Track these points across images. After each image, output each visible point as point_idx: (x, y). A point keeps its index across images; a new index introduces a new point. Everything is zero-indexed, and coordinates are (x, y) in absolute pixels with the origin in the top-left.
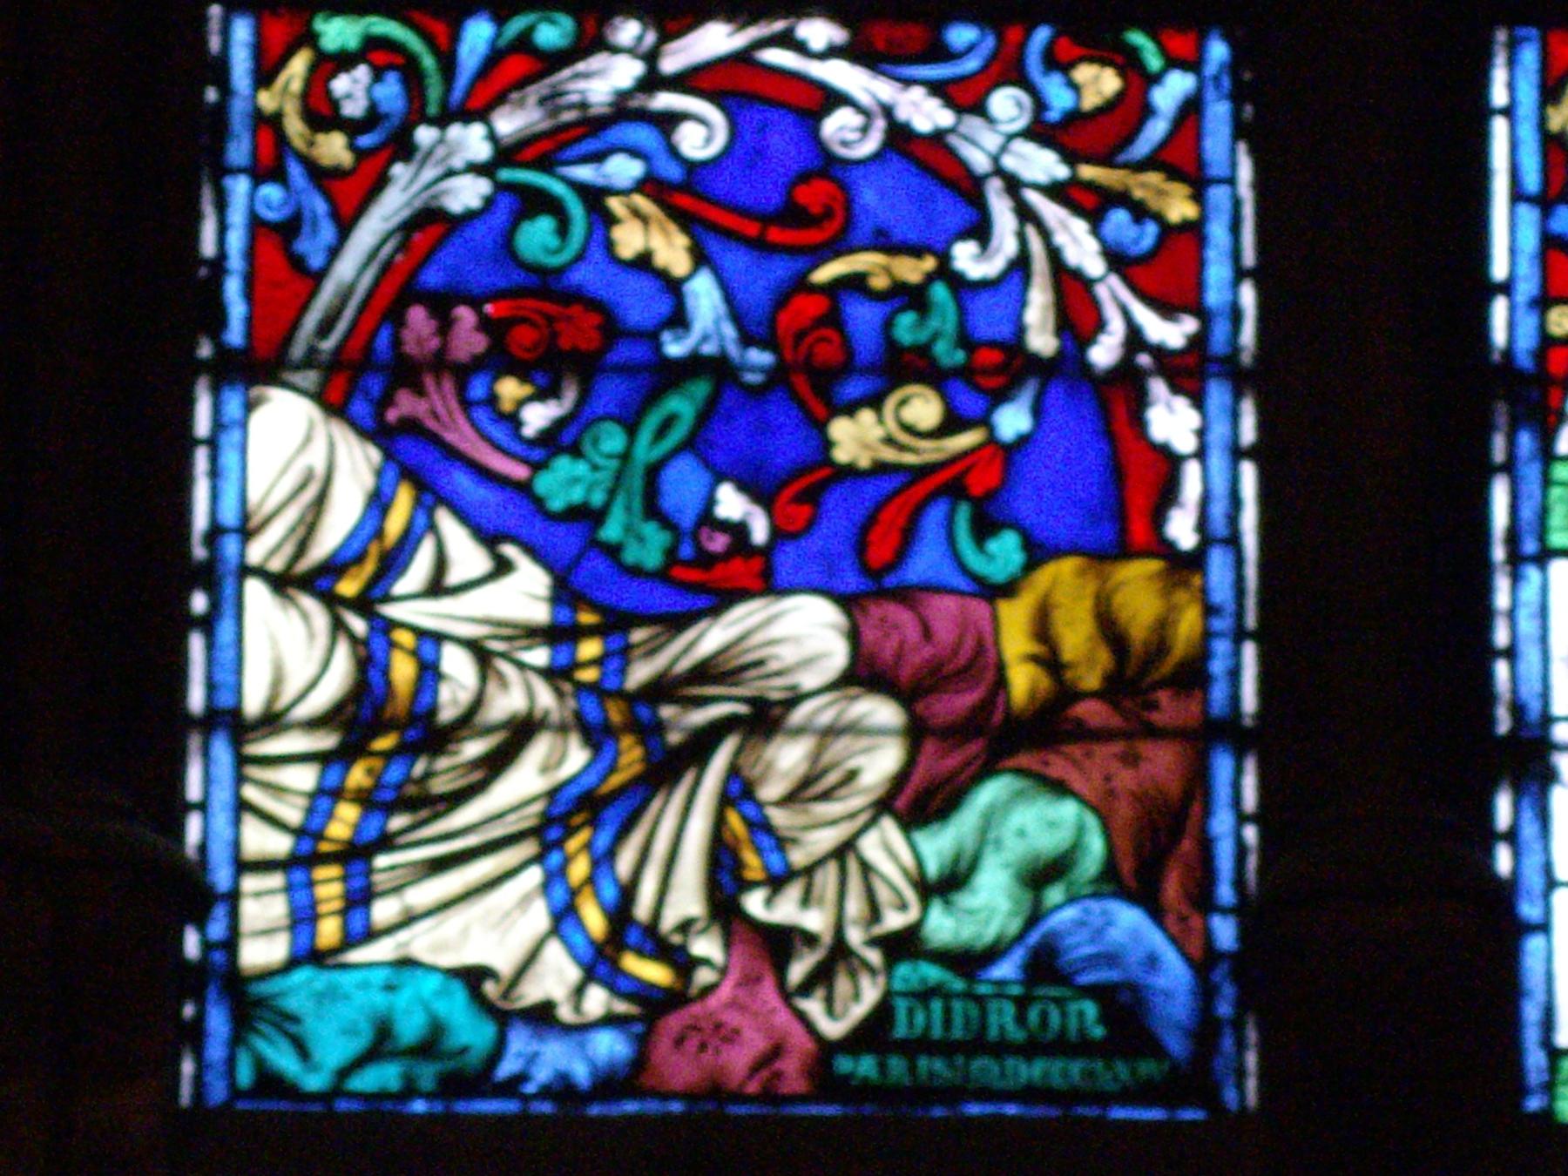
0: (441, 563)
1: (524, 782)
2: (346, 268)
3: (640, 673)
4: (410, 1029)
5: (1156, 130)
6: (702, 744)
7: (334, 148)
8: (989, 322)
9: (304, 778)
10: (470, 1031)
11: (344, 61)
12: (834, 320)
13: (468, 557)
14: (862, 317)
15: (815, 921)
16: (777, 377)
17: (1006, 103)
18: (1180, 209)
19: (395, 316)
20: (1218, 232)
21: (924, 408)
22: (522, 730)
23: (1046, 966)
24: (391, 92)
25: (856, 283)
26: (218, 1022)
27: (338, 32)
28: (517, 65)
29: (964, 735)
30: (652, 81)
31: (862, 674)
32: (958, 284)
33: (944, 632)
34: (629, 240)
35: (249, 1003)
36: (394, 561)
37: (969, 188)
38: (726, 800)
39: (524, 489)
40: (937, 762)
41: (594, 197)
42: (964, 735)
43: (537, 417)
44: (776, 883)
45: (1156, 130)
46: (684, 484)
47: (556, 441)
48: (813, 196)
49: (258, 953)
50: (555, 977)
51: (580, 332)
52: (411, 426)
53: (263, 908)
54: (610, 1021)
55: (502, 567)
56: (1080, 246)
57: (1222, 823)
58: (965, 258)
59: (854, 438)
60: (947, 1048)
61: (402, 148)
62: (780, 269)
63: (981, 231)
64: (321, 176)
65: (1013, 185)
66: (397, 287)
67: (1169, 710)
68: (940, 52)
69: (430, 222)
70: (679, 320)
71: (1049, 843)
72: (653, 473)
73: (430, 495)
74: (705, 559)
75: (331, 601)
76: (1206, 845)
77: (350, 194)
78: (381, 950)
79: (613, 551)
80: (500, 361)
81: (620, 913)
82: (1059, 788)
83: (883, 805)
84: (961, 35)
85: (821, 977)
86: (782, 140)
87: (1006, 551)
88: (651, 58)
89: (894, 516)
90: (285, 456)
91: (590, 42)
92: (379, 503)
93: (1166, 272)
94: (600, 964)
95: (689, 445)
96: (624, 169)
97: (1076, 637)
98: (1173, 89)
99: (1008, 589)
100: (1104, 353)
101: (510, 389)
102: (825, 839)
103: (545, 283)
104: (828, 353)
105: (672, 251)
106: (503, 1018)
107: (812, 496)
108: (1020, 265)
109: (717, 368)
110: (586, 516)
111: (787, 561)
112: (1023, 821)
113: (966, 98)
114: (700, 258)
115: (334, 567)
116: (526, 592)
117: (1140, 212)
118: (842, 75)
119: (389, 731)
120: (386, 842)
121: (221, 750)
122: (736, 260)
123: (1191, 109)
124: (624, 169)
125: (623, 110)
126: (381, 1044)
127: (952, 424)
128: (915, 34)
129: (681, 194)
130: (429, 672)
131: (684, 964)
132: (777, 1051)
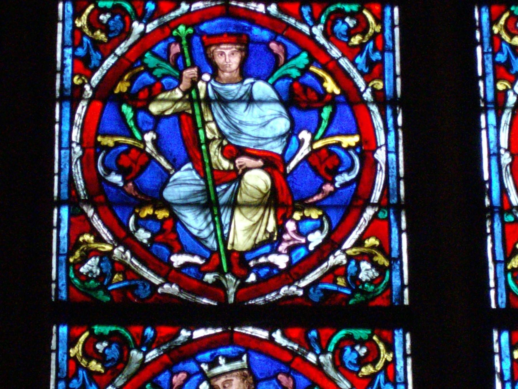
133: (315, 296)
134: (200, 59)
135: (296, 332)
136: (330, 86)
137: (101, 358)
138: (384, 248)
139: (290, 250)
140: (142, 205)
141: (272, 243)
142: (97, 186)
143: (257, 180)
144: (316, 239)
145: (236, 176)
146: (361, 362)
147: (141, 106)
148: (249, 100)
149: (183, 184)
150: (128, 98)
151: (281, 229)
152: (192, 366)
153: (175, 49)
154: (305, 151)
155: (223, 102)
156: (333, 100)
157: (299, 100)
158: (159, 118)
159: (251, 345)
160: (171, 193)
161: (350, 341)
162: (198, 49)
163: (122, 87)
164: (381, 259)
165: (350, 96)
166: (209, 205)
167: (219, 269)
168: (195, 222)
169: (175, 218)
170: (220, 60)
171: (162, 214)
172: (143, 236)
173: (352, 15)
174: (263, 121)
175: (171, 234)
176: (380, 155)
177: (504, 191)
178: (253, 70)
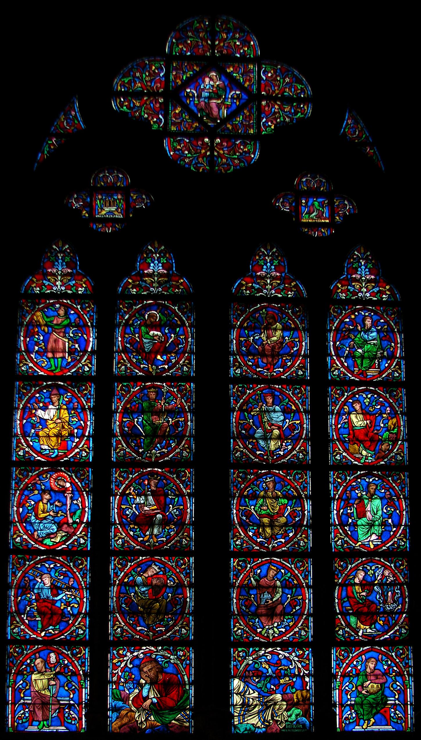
0: (249, 692)
1: (256, 709)
2: (241, 669)
3: (265, 700)
4: (248, 728)
5: (305, 656)
6: (270, 706)
7: (240, 659)
8: (292, 671)
9: (239, 709)
10: (253, 729)
11: (240, 652)
12: (280, 672)
13: (251, 692)
14: (282, 671)
15: (279, 719)
16: (276, 677)
17: (293, 654)
18: (307, 662)
19: (245, 673)
20: (310, 664)
21: (287, 679)
22: (256, 705)
23: (298, 722)
24: (244, 654)
25: (282, 669)
26: (233, 728)
27: (240, 649)
28: (254, 652)
29: (291, 705)
30: (265, 653)
31: (283, 700)
32: (290, 669)
33: (289, 697)
34: (264, 666)
35: (235, 727)
36: (246, 692)
37: (291, 661)
38: (272, 710)
39: (256, 686)
40: (289, 707)
41: (261, 662)
42: (291, 705)
43: (257, 680)
44: (276, 717)
45: (305, 656)
46: (268, 685)
47: (258, 682)
48: (278, 662)
49: (236, 723)
50: (259, 724)
51: (260, 674)
52: (247, 681)
53: (236, 719)
54: (264, 727)
55: (254, 692)
56: (300, 666)
57: (311, 711)
58: (290, 666)
59: (282, 681)
60: (290, 729)
61: (245, 659)
62: (276, 668)
63: (292, 665)
64: (239, 661)
65: (294, 661)
66: (245, 670)
67: (307, 702)
68: (289, 650)
69: (248, 664)
70: (268, 672)
71: (298, 713)
72: (266, 684)
73: (248, 687)
74: (270, 691)
75: (241, 695)
76: (310, 712)
77: (241, 662)
78: (246, 722)
79: (263, 691)
80: (253, 676)
81: (264, 719)
82: (299, 709)
83: (285, 710)
84: (290, 649)
85: (280, 724)
86: (276, 658)
87: (294, 690)
88: (265, 651)
89: (285, 688)
90: (236, 683)
91: (260, 650)
92: (244, 687)
93: (306, 667)
94: (263, 723)
95: (269, 682)
96: (263, 660)
97: (299, 697)
98: (307, 652)
99: (294, 693)
100: (301, 674)
101: (254, 678)
102: (280, 713)
103: (257, 669)
104: (280, 675)
105: (267, 667)
106: (255, 728)
107: (279, 686)
108: (295, 667)
109: (271, 676)
110: (261, 688)
111: (277, 691)
112: (296, 711)
113: (290, 654)
114: (269, 667)
115: (241, 692)
116: (256, 694)
117: (304, 663)
118: (280, 652)
119: (246, 706)
120: (246, 714)
121: (232, 707)
122: (272, 667)
123: (308, 654)
124: (263, 660)
125: (263, 655)
126: (246, 730)
127: (290, 680)
128: (286, 649)
129: (268, 662)
130: (249, 701)
131: (269, 723)
132: (277, 729)
133: (289, 462)
134: (263, 400)
135: (285, 471)
136: (293, 407)
137: (241, 478)
138: (305, 450)
139: (284, 450)
140: (250, 439)
141: (279, 448)
142: (239, 433)
143: (276, 432)
144: (290, 447)
145: (271, 431)
146: (300, 479)
147: (249, 413)
148: (274, 411)
149: (259, 432)
150: (246, 410)
151: (282, 445)
152: (261, 480)
153: (257, 397)
154: (287, 425)
155: (268, 411)
156: (294, 412)
157: (286, 411)
158: (254, 415)
159: (275, 475)
160: (257, 435)
161: (297, 473)
162: (263, 398)
163: (245, 408)
164: (304, 453)
165: (298, 410)
166: (265, 438)
167: (267, 455)
168: (262, 443)
169: (257, 442)
170: (268, 400)
171: (254, 441)
172: (250, 446)
173: (299, 389)
174: (278, 417)
175: (256, 447)
176: (305, 426)
177: (333, 435)
178: (275, 403)
